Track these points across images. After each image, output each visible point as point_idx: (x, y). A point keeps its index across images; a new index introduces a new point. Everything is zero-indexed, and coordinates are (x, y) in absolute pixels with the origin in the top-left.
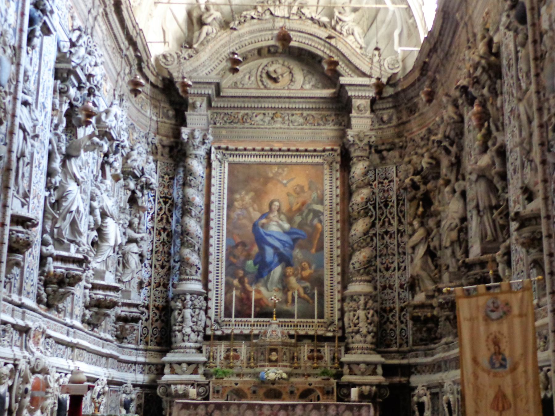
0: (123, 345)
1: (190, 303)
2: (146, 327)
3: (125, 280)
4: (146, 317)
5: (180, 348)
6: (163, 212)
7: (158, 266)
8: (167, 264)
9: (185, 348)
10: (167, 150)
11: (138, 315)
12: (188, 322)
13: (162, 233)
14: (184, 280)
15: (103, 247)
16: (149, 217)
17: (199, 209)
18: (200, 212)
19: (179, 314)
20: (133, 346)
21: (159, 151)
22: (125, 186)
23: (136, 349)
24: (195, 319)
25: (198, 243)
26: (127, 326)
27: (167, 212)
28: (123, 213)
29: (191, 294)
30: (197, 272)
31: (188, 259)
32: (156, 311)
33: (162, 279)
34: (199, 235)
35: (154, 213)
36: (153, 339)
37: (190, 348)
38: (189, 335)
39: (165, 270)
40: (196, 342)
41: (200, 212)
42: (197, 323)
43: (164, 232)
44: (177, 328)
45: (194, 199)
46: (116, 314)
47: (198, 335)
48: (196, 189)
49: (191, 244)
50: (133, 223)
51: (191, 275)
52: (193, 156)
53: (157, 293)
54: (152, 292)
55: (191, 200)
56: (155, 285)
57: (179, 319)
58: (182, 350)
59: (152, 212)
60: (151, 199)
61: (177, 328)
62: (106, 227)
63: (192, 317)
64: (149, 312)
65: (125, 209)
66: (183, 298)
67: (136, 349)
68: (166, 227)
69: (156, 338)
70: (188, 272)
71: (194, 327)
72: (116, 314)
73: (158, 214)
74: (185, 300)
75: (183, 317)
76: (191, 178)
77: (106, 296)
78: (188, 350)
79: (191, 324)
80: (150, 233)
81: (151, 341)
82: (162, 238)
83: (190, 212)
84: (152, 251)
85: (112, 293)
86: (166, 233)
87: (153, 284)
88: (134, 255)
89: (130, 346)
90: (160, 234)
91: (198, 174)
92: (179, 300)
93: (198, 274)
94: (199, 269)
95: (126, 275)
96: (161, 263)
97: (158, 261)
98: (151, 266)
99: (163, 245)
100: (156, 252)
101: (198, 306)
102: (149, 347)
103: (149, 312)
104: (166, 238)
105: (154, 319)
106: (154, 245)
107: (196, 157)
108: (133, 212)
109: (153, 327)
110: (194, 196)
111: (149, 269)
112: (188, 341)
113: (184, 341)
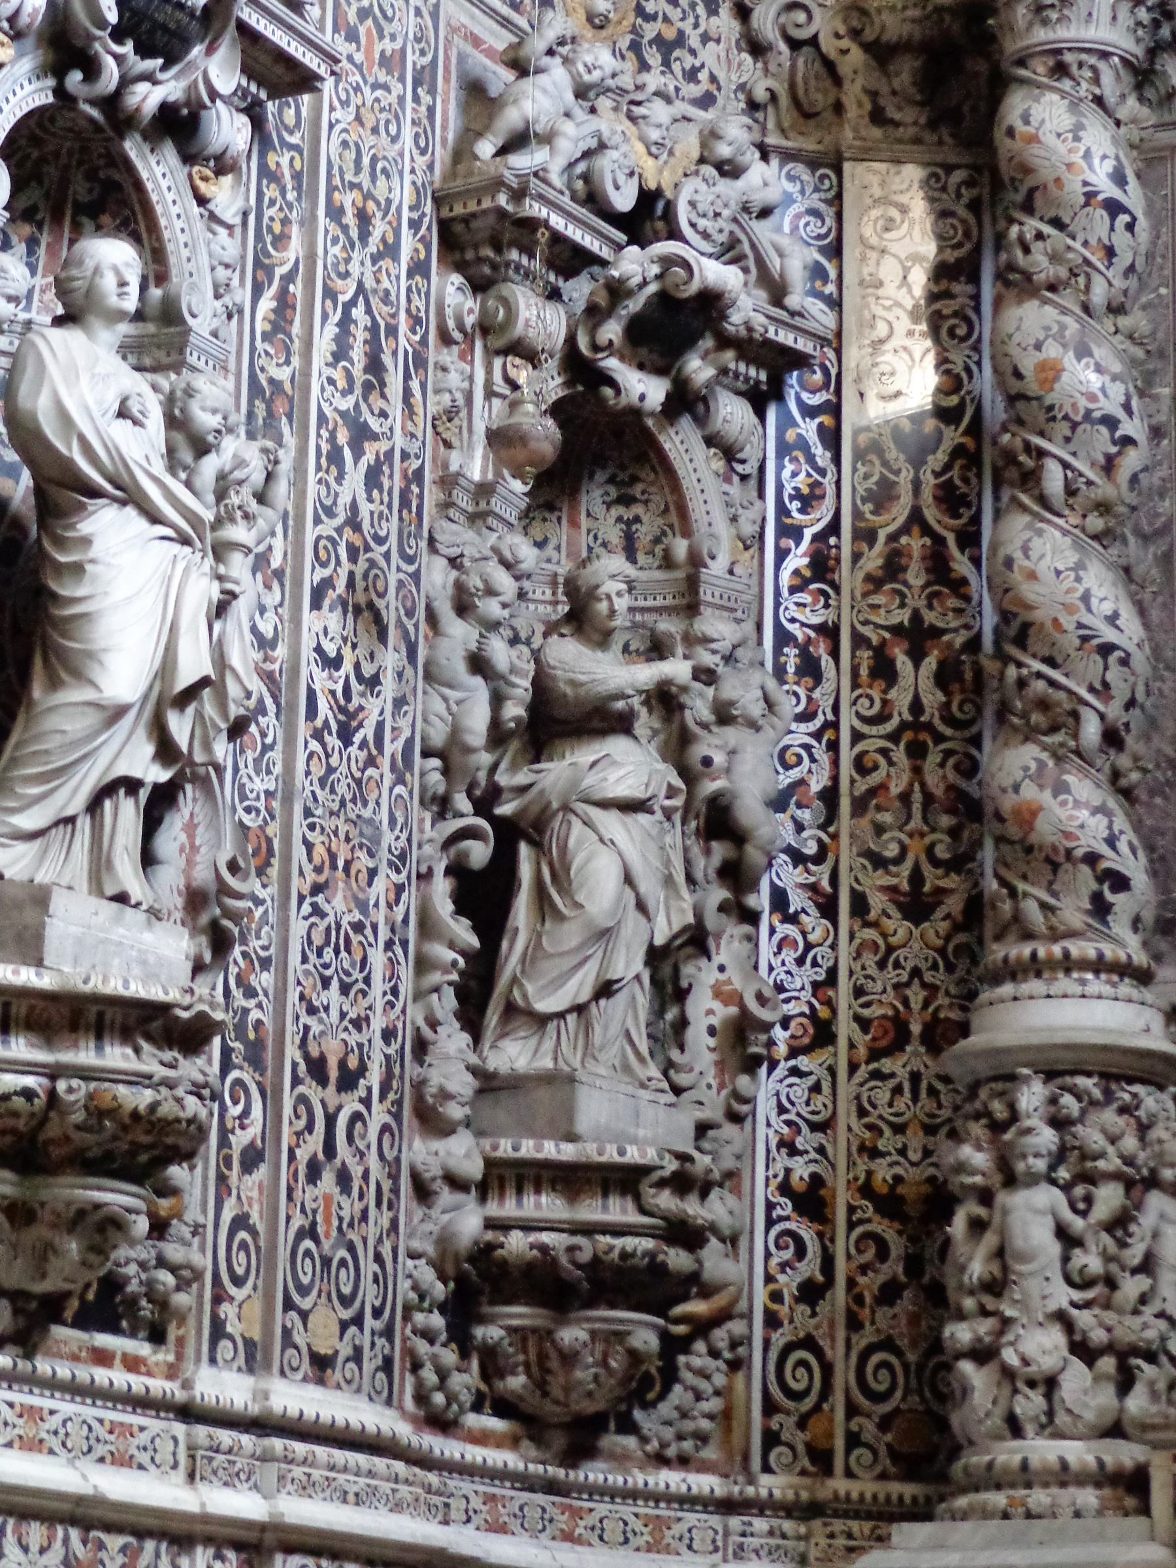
0: (594, 1473)
1: (1047, 1137)
2: (809, 1343)
3: (544, 1006)
4: (810, 1267)
5: (993, 1479)
6: (900, 513)
7: (877, 902)
8: (952, 881)
9: (1025, 1475)
10: (905, 72)
11: (648, 1244)
12: (1033, 1286)
13: (903, 663)
14: (1013, 972)
15: (53, 722)
16: (798, 559)
17: (1101, 441)
18: (1109, 466)
19: (978, 1226)
20: (705, 1483)
21: (853, 94)
22: (485, 328)
23: (728, 1506)
24: (1090, 1261)
25: (1104, 690)
26: (571, 1335)
27: (931, 514)
28: (476, 518)
29: (1050, 1075)
30: (1101, 909)
31: (1028, 816)
32: (880, 1226)
33: (916, 996)
34: (1109, 635)
35: (834, 527)
36: (868, 1428)
37: (1064, 1476)
38: (1050, 1384)
39: (936, 927)
40: (1115, 1430)
41: (1109, 466)
42: (1111, 1283)
43: (917, 657)
44: (961, 1333)
45: (1051, 372)
46: (444, 1240)
47: (1125, 1383)
48: (1067, 299)
49: (1044, 705)
50: (592, 593)
51: (1055, 935)
52: (1040, 68)
53: (883, 1095)
54: (846, 1090)
55: (1032, 386)
56: (863, 1041)
57: (978, 1268)
58: (998, 1499)
59: (814, 523)
60: (809, 429)
61: (961, 1333)
62: (78, 569)
63: (1067, 1239)
64: (826, 1240)
65: (484, 490)
66: (998, 1109)
67: (728, 1506)
68: (930, 617)
69: (884, 1424)
70: (1031, 908)
71: (1084, 1319)
72: (444, 1240)
73: (866, 535)
74: (1014, 1116)
75: (1000, 1253)
76: (1032, 225)
77: (54, 1073)
78: (1039, 1498)
79: (1062, 1296)
80: (810, 669)
81: (853, 1441)
82: (901, 698)
83: (1030, 479)
84: (830, 796)
85: (117, 1056)
86: (930, 663)
87: (845, 1028)
88: (611, 823)
89: (671, 1479)
90: (884, 671)
91: (1074, 189)
92: (977, 1129)
93: (1120, 926)
94: (1120, 883)
95: (551, 969)
96: (901, 877)
97: (879, 862)
98: (828, 909)
99: (917, 752)
100: (860, 806)
101: (1111, 1163)
102: (839, 1485)
103: (826, 1240)
104: (932, 698)
105: (869, 1284)
106: (847, 755)
107: (1061, 70)
108: (645, 532)
109: (861, 1341)
110: (1052, 350)
111: (813, 921)
112: (1048, 1425)
113: (1014, 1427)
